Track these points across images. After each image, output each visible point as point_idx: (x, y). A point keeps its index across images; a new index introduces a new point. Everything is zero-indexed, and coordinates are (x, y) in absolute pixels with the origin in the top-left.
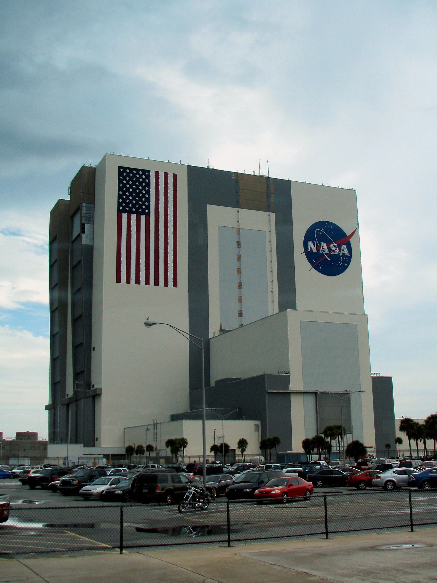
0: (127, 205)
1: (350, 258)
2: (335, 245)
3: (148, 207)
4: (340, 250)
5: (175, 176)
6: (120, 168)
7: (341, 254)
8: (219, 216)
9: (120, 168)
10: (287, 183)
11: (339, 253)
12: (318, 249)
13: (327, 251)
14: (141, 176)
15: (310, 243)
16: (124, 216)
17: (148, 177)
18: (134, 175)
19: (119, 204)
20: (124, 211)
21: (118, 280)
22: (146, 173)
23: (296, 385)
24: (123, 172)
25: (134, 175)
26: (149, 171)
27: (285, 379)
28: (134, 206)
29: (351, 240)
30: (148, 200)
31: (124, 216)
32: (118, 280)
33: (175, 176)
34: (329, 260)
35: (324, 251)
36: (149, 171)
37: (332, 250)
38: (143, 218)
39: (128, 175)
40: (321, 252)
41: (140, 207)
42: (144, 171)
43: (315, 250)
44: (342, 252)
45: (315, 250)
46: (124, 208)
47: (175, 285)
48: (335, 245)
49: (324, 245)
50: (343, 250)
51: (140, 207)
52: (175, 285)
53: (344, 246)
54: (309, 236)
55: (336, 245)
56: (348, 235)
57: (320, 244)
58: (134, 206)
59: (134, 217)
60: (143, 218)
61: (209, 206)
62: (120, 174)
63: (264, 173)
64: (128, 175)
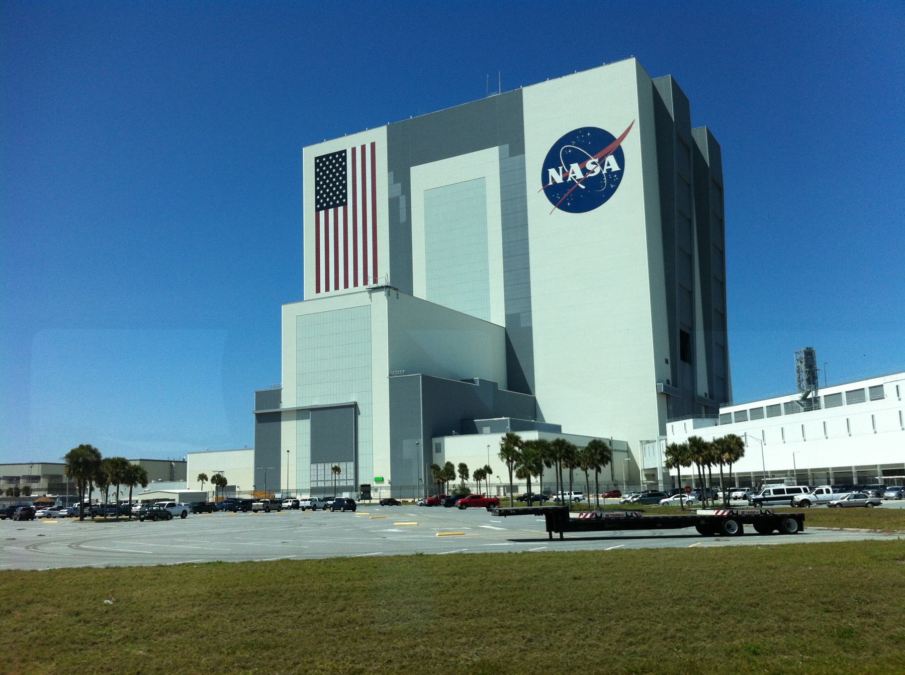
0: (325, 201)
1: (620, 174)
2: (593, 160)
3: (345, 196)
4: (602, 166)
5: (373, 145)
6: (316, 159)
7: (604, 172)
9: (316, 159)
12: (565, 178)
13: (579, 175)
14: (337, 160)
15: (552, 172)
16: (322, 213)
17: (345, 159)
18: (331, 162)
19: (317, 202)
20: (322, 208)
21: (318, 291)
22: (342, 154)
23: (288, 402)
24: (320, 162)
25: (331, 162)
26: (345, 151)
27: (275, 395)
28: (331, 198)
29: (624, 145)
31: (322, 213)
32: (318, 291)
33: (373, 145)
34: (583, 187)
35: (575, 177)
36: (345, 151)
37: (589, 171)
38: (341, 209)
39: (324, 163)
40: (569, 179)
41: (337, 196)
42: (340, 153)
44: (606, 167)
45: (559, 179)
46: (321, 204)
48: (593, 160)
49: (575, 167)
50: (609, 165)
51: (338, 198)
53: (611, 159)
54: (552, 161)
55: (596, 160)
56: (617, 136)
57: (569, 169)
59: (331, 211)
60: (341, 209)
61: (412, 168)
62: (317, 165)
64: (324, 165)
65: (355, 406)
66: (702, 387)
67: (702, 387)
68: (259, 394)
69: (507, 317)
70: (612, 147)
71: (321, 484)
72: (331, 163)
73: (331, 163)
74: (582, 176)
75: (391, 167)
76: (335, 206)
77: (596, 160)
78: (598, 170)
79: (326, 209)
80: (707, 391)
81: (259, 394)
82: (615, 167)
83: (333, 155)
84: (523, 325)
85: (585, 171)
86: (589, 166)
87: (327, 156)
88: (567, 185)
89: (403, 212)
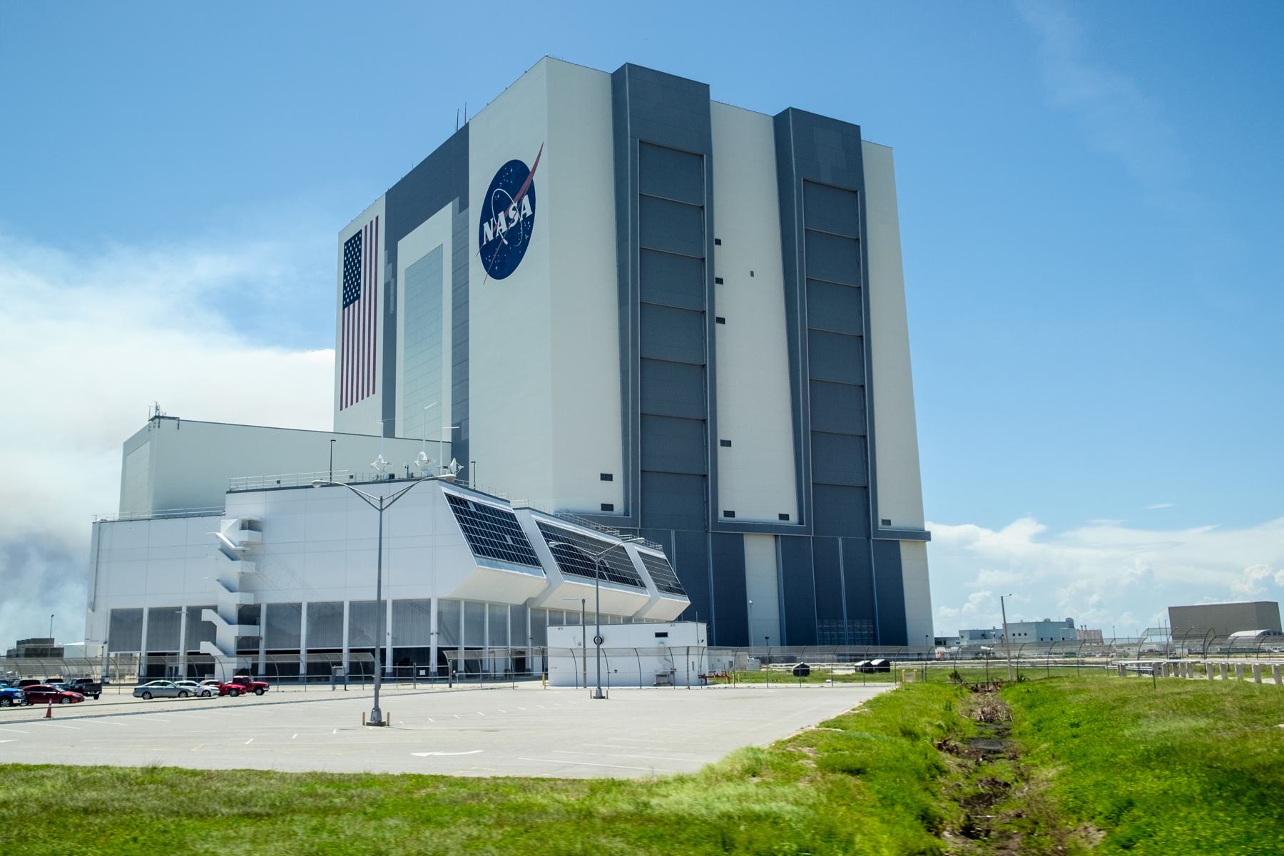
1: (532, 218)
12: (495, 234)
15: (486, 225)
17: (360, 239)
43: (491, 238)
49: (501, 215)
53: (526, 200)
70: (526, 185)
74: (505, 229)
76: (353, 301)
77: (515, 204)
82: (529, 213)
84: (463, 438)
85: (508, 220)
86: (512, 214)
88: (497, 240)
89: (392, 298)
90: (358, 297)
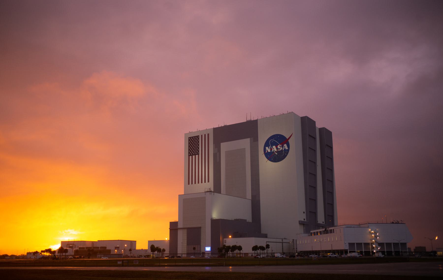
1: (288, 150)
3: (199, 151)
5: (208, 135)
8: (225, 146)
10: (256, 121)
11: (282, 150)
13: (276, 150)
15: (267, 148)
17: (199, 139)
19: (189, 153)
21: (189, 184)
22: (198, 137)
23: (180, 226)
26: (199, 136)
28: (194, 152)
30: (199, 148)
31: (191, 157)
32: (189, 184)
33: (208, 135)
36: (199, 136)
38: (197, 156)
42: (197, 136)
43: (269, 151)
45: (269, 151)
47: (208, 181)
49: (274, 147)
52: (208, 181)
53: (285, 145)
54: (267, 144)
58: (194, 152)
59: (194, 156)
60: (197, 156)
61: (222, 144)
62: (189, 140)
63: (249, 119)
65: (200, 228)
66: (321, 219)
67: (321, 219)
68: (171, 223)
69: (252, 196)
71: (190, 252)
72: (194, 140)
73: (194, 140)
75: (214, 143)
78: (281, 149)
79: (192, 156)
80: (324, 221)
81: (171, 223)
82: (287, 148)
83: (195, 137)
86: (279, 147)
87: (193, 137)
88: (272, 153)
90: (198, 154)
